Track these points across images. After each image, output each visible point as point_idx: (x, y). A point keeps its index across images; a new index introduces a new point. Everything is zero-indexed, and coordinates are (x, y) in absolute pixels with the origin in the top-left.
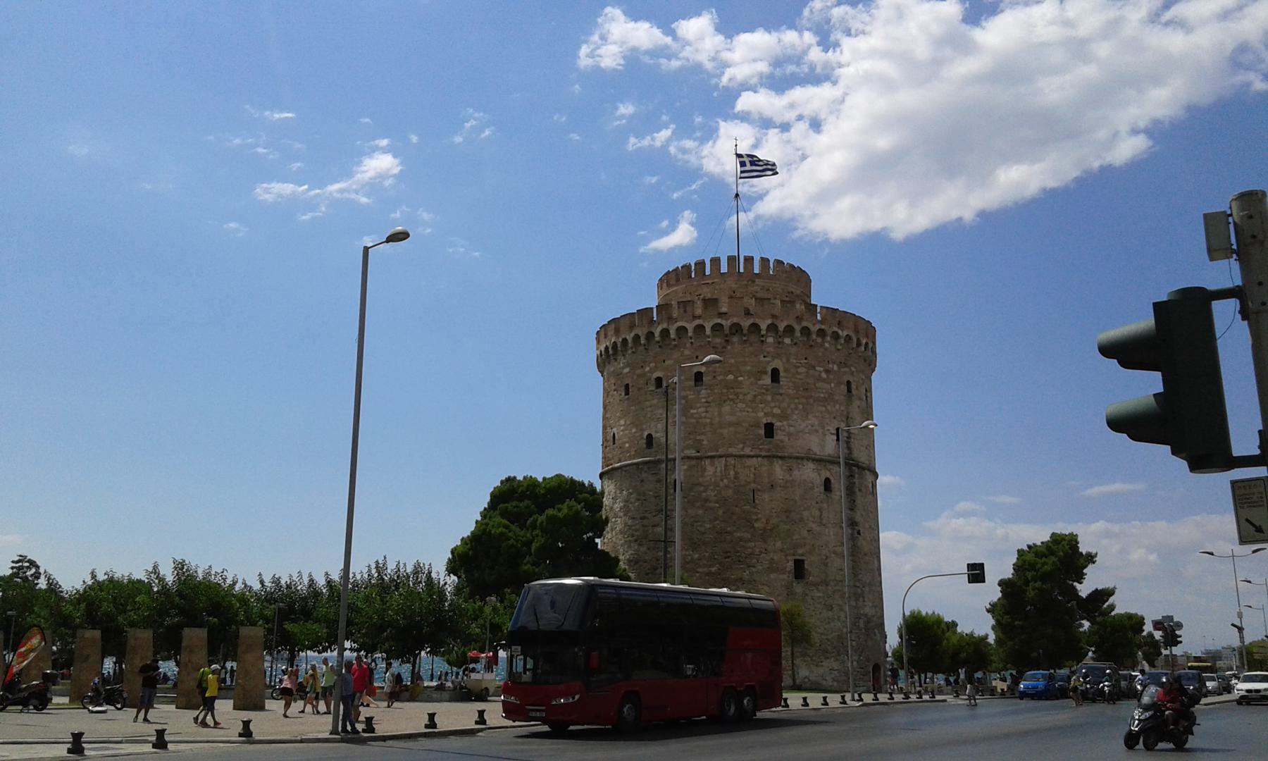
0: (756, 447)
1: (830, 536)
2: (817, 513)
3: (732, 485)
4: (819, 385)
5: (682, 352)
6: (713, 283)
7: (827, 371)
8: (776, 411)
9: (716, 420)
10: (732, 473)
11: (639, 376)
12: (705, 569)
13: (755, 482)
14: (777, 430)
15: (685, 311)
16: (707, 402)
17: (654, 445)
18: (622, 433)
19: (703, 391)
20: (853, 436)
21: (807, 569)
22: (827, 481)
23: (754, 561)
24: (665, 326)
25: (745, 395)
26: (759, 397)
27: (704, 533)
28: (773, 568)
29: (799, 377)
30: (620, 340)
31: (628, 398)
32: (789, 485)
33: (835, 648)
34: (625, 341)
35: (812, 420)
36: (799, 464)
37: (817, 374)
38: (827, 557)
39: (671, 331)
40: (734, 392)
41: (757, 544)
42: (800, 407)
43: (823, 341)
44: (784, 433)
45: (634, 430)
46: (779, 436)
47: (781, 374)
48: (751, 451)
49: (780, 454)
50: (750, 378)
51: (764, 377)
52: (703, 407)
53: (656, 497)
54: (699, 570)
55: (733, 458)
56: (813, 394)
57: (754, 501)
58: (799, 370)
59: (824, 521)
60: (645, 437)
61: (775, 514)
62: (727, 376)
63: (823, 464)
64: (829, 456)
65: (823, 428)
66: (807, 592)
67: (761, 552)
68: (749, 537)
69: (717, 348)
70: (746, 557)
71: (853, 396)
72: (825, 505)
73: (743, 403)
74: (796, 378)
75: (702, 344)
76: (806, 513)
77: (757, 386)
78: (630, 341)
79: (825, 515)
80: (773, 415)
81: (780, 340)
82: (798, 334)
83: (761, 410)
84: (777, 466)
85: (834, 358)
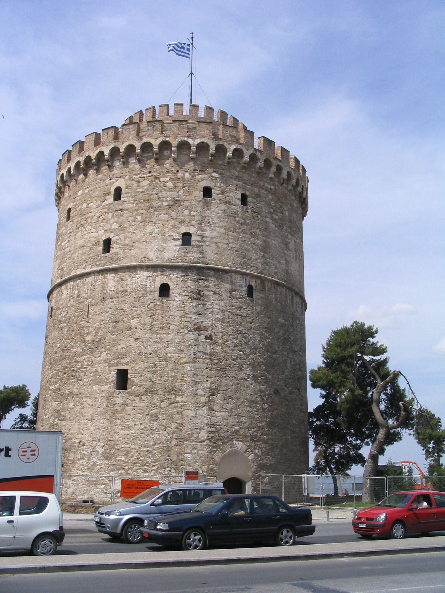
2: (149, 320)
8: (115, 226)
10: (76, 292)
13: (91, 297)
23: (83, 374)
29: (141, 190)
32: (119, 295)
33: (157, 461)
41: (85, 357)
44: (119, 246)
47: (122, 192)
51: (108, 197)
57: (88, 317)
58: (142, 184)
61: (103, 326)
64: (169, 260)
66: (128, 401)
76: (134, 322)
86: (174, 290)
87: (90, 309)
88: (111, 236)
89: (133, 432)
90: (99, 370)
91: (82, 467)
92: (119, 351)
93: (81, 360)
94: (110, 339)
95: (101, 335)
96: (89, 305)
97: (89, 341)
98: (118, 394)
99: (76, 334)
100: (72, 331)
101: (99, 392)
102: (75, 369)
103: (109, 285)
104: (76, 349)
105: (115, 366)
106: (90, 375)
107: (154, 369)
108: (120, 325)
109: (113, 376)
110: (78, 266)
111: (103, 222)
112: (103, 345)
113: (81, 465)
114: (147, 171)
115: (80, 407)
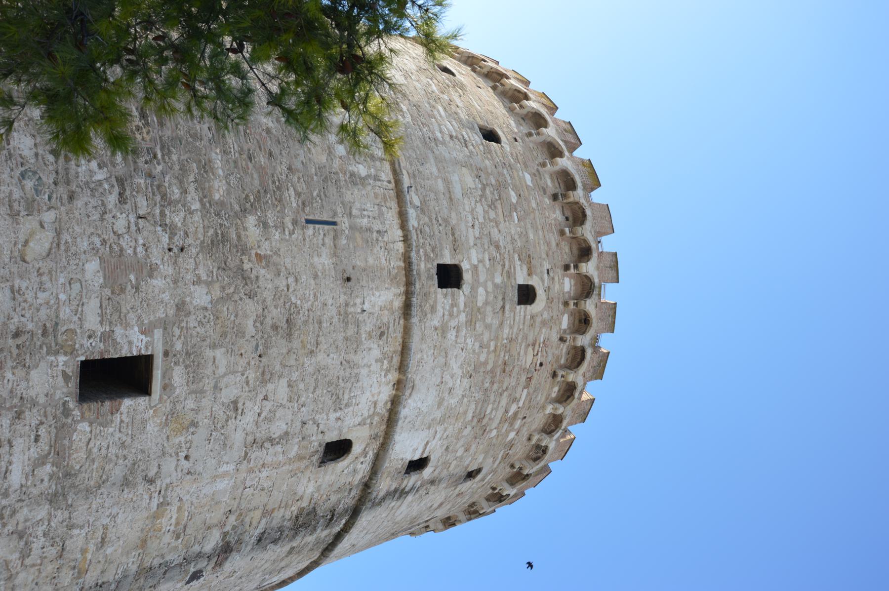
0: (421, 241)
1: (215, 478)
13: (352, 228)
14: (453, 295)
36: (390, 362)
38: (151, 481)
41: (197, 217)
46: (442, 297)
55: (391, 177)
57: (308, 222)
62: (513, 189)
66: (31, 417)
67: (172, 230)
68: (217, 197)
70: (150, 175)
76: (280, 389)
80: (474, 289)
87: (326, 227)
90: (154, 282)
92: (209, 353)
93: (189, 198)
94: (246, 316)
95: (261, 279)
96: (334, 223)
98: (64, 373)
99: (261, 170)
101: (76, 287)
102: (159, 168)
103: (377, 294)
104: (220, 172)
105: (165, 343)
106: (141, 241)
107: (139, 479)
108: (279, 347)
109: (130, 343)
111: (490, 260)
112: (232, 290)
115: (17, 194)
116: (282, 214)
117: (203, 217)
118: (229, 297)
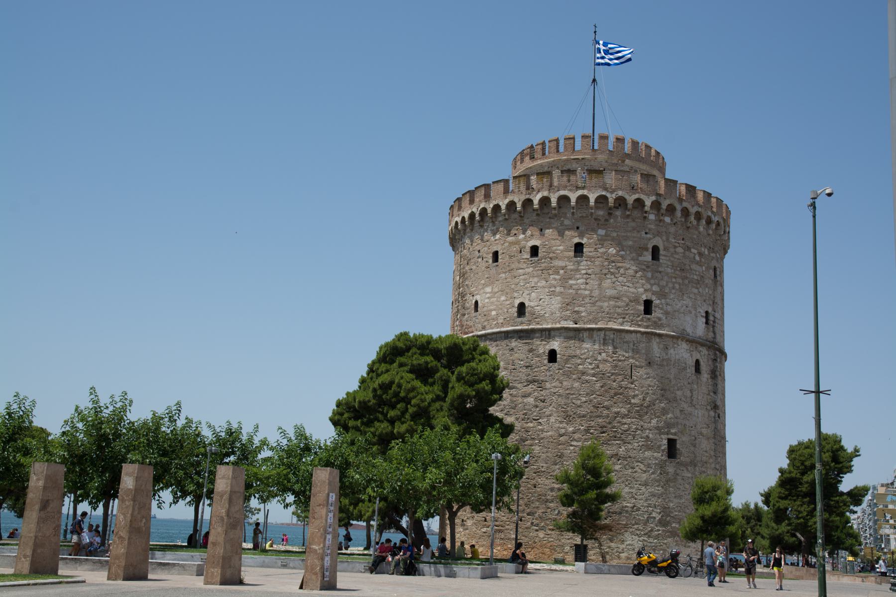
1: (698, 417)
2: (688, 394)
3: (609, 359)
4: (694, 266)
5: (563, 221)
6: (583, 159)
7: (700, 254)
9: (596, 293)
11: (511, 244)
12: (580, 444)
15: (569, 181)
16: (587, 274)
17: (527, 314)
18: (487, 301)
19: (585, 263)
20: (717, 321)
21: (679, 450)
22: (697, 362)
24: (546, 194)
25: (627, 269)
26: (640, 273)
27: (580, 406)
28: (648, 446)
30: (491, 206)
31: (497, 266)
34: (497, 208)
35: (688, 301)
37: (692, 255)
39: (552, 200)
40: (615, 265)
41: (633, 420)
42: (677, 286)
43: (698, 225)
45: (503, 298)
46: (657, 313)
47: (661, 252)
48: (631, 326)
49: (658, 331)
50: (631, 253)
51: (645, 253)
52: (582, 278)
53: (527, 367)
54: (572, 443)
55: (612, 332)
56: (688, 276)
59: (694, 403)
60: (516, 306)
61: (651, 391)
63: (694, 344)
64: (700, 337)
65: (695, 309)
66: (678, 471)
69: (599, 220)
71: (717, 281)
72: (695, 386)
73: (625, 278)
74: (675, 258)
75: (584, 215)
76: (679, 393)
77: (638, 262)
78: (503, 207)
79: (695, 396)
81: (662, 218)
82: (678, 214)
83: (641, 286)
84: (655, 343)
85: (705, 241)
86: (704, 367)
88: (654, 298)
89: (683, 501)
91: (638, 532)
96: (632, 366)
97: (635, 404)
99: (616, 394)
100: (610, 388)
102: (620, 430)
105: (665, 434)
109: (665, 445)
110: (610, 319)
111: (642, 280)
113: (636, 530)
114: (682, 237)
116: (630, 388)
117: (633, 418)
118: (654, 412)
